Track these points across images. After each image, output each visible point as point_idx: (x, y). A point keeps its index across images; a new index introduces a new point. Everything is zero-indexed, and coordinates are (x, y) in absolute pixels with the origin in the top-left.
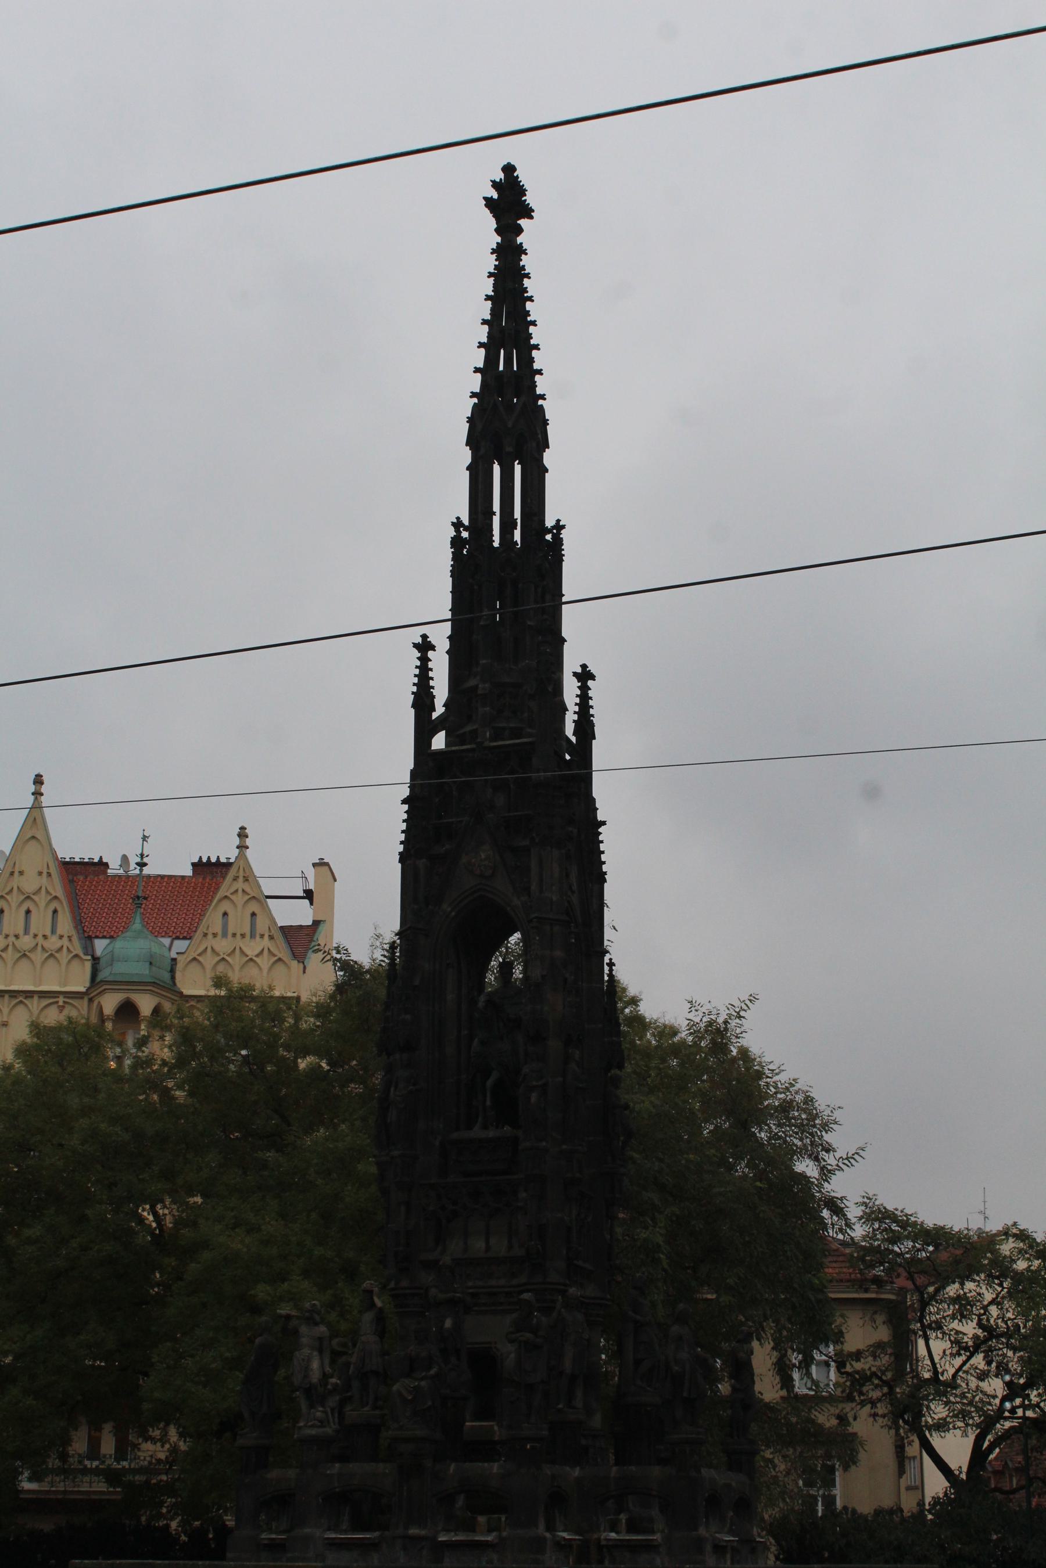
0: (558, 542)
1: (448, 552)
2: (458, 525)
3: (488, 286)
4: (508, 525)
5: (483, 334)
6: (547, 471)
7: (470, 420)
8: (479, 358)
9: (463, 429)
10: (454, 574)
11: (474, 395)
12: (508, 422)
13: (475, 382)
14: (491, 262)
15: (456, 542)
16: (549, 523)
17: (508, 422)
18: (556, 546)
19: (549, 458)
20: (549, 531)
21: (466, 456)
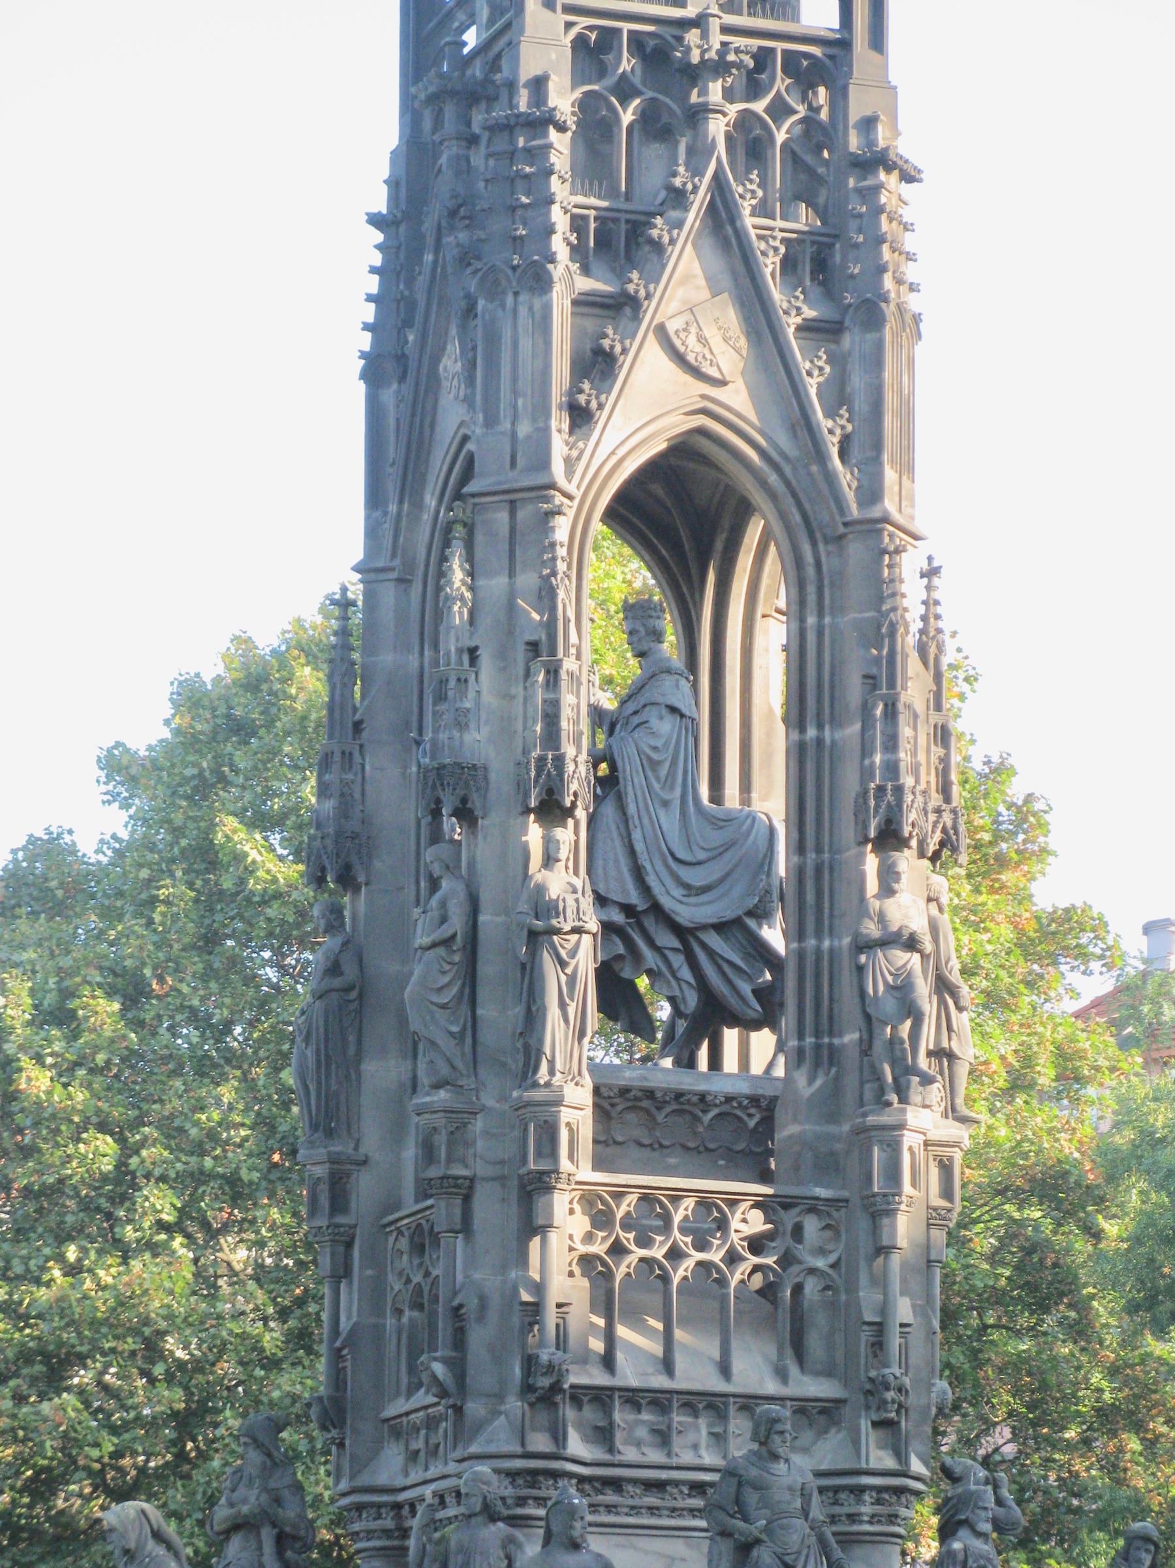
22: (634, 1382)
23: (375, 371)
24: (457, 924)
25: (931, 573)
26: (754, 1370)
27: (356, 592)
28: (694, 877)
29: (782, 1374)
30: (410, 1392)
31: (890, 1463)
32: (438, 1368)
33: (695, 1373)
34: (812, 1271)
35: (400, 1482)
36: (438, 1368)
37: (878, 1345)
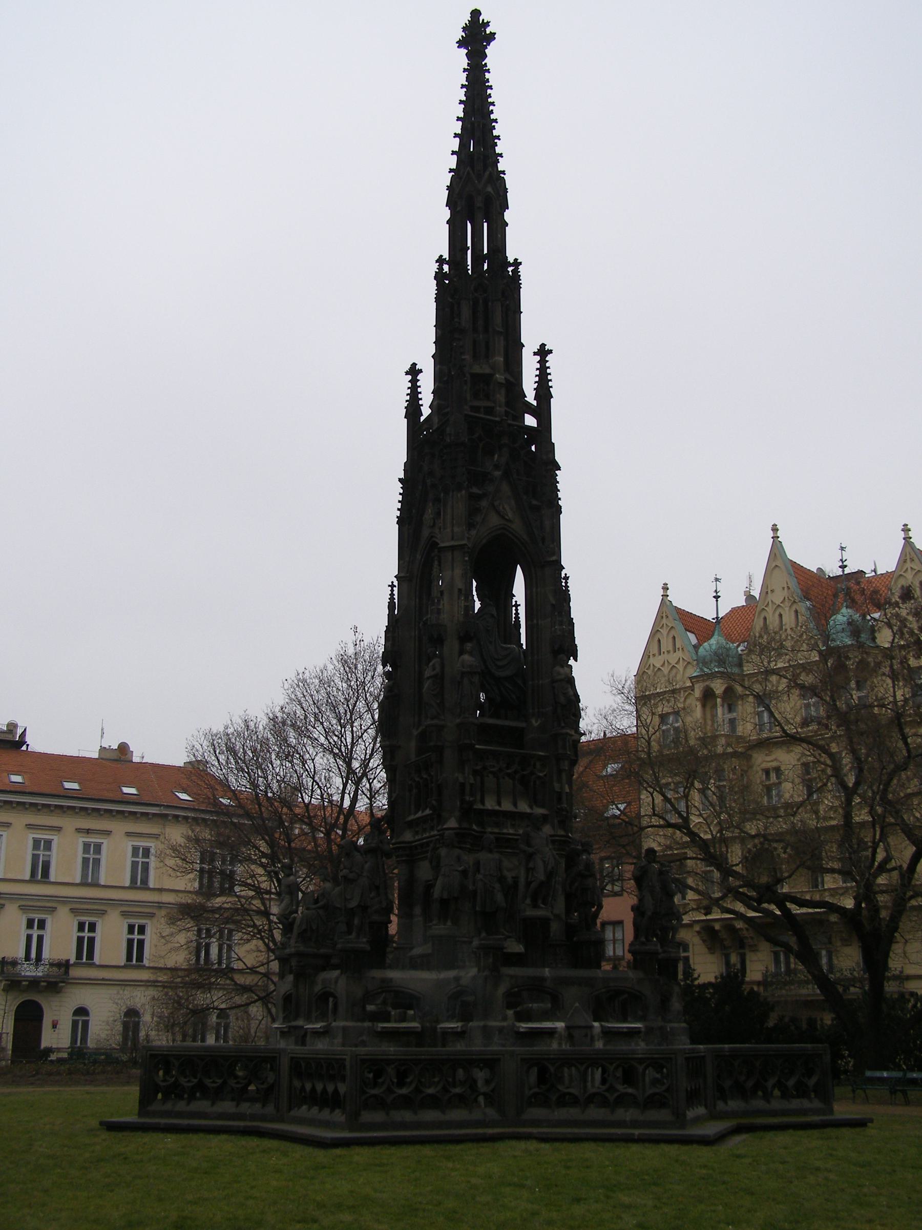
0: (516, 271)
1: (432, 286)
2: (440, 260)
3: (461, 95)
4: (478, 258)
5: (458, 127)
6: (507, 225)
7: (449, 188)
8: (455, 144)
9: (444, 195)
10: (438, 300)
11: (451, 171)
12: (477, 190)
13: (453, 162)
14: (462, 78)
15: (439, 276)
16: (511, 259)
17: (477, 190)
18: (516, 277)
19: (508, 215)
20: (511, 265)
21: (447, 214)
22: (490, 808)
23: (400, 521)
24: (438, 670)
25: (566, 578)
26: (524, 807)
27: (396, 583)
28: (500, 663)
29: (531, 807)
30: (416, 813)
31: (562, 833)
32: (434, 802)
33: (507, 806)
34: (539, 777)
35: (412, 839)
36: (434, 802)
37: (559, 800)
